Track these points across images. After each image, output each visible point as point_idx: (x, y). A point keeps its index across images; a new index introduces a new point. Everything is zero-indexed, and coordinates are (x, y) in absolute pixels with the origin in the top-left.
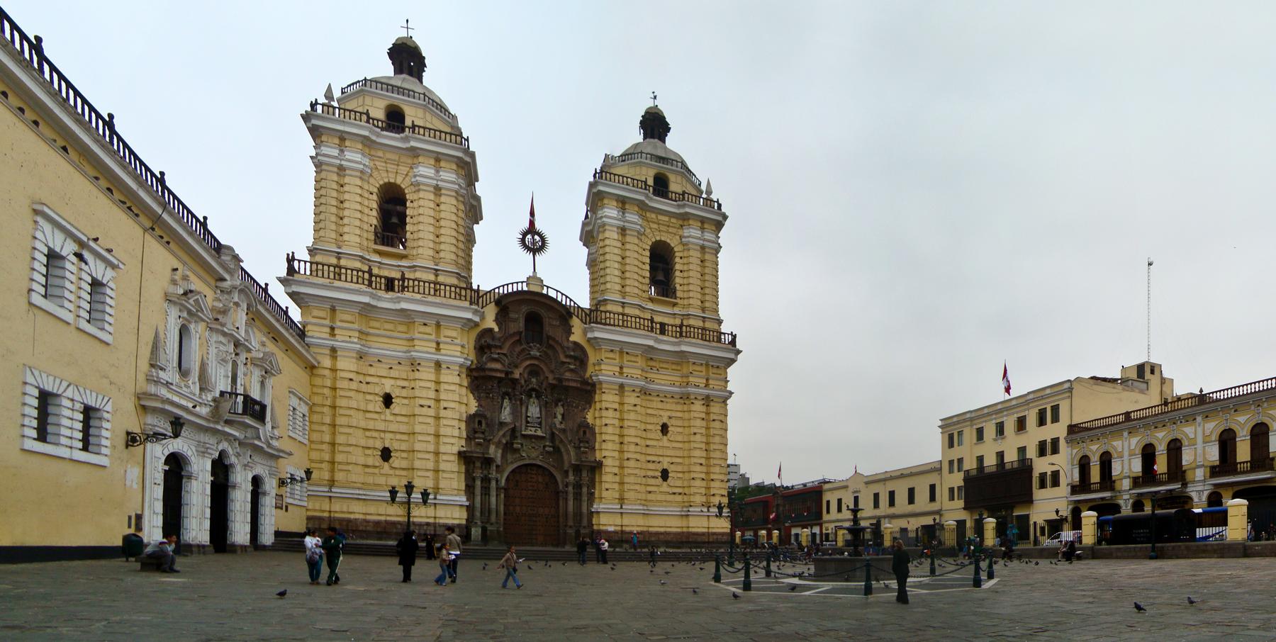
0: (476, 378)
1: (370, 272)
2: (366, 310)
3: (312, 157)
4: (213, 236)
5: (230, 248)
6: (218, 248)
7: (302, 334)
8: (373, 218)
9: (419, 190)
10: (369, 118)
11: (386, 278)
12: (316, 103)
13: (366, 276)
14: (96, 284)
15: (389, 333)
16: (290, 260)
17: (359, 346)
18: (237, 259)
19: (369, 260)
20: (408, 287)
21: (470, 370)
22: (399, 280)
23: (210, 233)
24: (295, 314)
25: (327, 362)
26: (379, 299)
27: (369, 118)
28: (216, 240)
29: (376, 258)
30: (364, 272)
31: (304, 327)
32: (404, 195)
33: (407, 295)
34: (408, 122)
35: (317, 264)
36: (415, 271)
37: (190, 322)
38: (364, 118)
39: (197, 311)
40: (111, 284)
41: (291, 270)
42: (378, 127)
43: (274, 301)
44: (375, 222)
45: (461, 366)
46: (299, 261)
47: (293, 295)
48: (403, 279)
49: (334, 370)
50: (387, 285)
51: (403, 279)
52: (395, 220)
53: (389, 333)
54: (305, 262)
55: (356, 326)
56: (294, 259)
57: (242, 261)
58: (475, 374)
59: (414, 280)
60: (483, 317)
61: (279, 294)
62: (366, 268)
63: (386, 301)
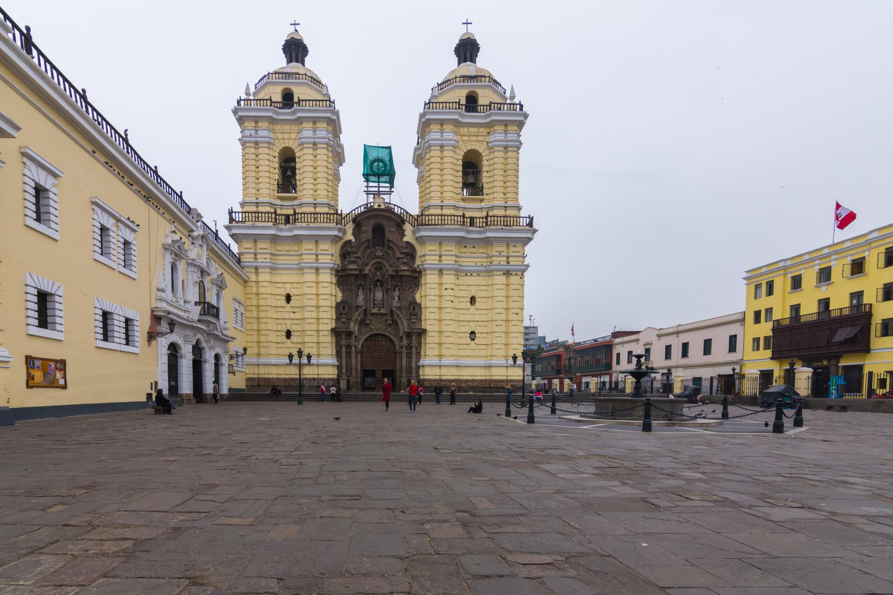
0: (341, 276)
1: (275, 213)
2: (274, 239)
3: (239, 140)
4: (186, 204)
5: (196, 210)
6: (189, 210)
7: (239, 261)
8: (276, 175)
9: (303, 149)
10: (272, 102)
11: (284, 215)
12: (241, 100)
13: (273, 216)
14: (126, 243)
15: (288, 253)
16: (231, 213)
17: (271, 264)
18: (199, 216)
19: (275, 205)
20: (298, 219)
21: (337, 271)
22: (292, 215)
23: (184, 202)
24: (235, 248)
25: (253, 277)
26: (281, 230)
27: (272, 102)
28: (188, 206)
29: (279, 202)
30: (272, 213)
31: (240, 256)
32: (294, 153)
33: (298, 224)
34: (296, 100)
35: (245, 212)
36: (302, 207)
37: (176, 260)
38: (269, 102)
39: (180, 252)
40: (134, 242)
41: (232, 220)
42: (277, 107)
43: (222, 241)
44: (277, 177)
45: (331, 269)
46: (235, 212)
47: (233, 236)
48: (295, 213)
49: (257, 282)
50: (285, 220)
51: (295, 213)
52: (289, 173)
53: (288, 253)
54: (239, 212)
55: (268, 251)
56: (232, 212)
57: (202, 217)
58: (341, 274)
59: (301, 214)
60: (344, 232)
61: (224, 236)
62: (273, 211)
63: (286, 231)
